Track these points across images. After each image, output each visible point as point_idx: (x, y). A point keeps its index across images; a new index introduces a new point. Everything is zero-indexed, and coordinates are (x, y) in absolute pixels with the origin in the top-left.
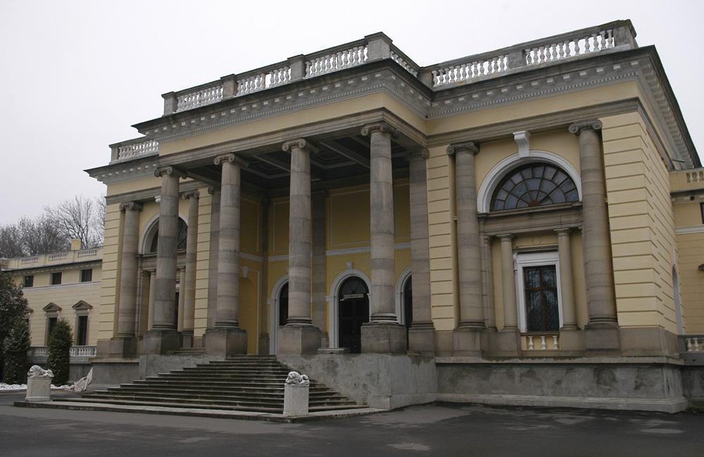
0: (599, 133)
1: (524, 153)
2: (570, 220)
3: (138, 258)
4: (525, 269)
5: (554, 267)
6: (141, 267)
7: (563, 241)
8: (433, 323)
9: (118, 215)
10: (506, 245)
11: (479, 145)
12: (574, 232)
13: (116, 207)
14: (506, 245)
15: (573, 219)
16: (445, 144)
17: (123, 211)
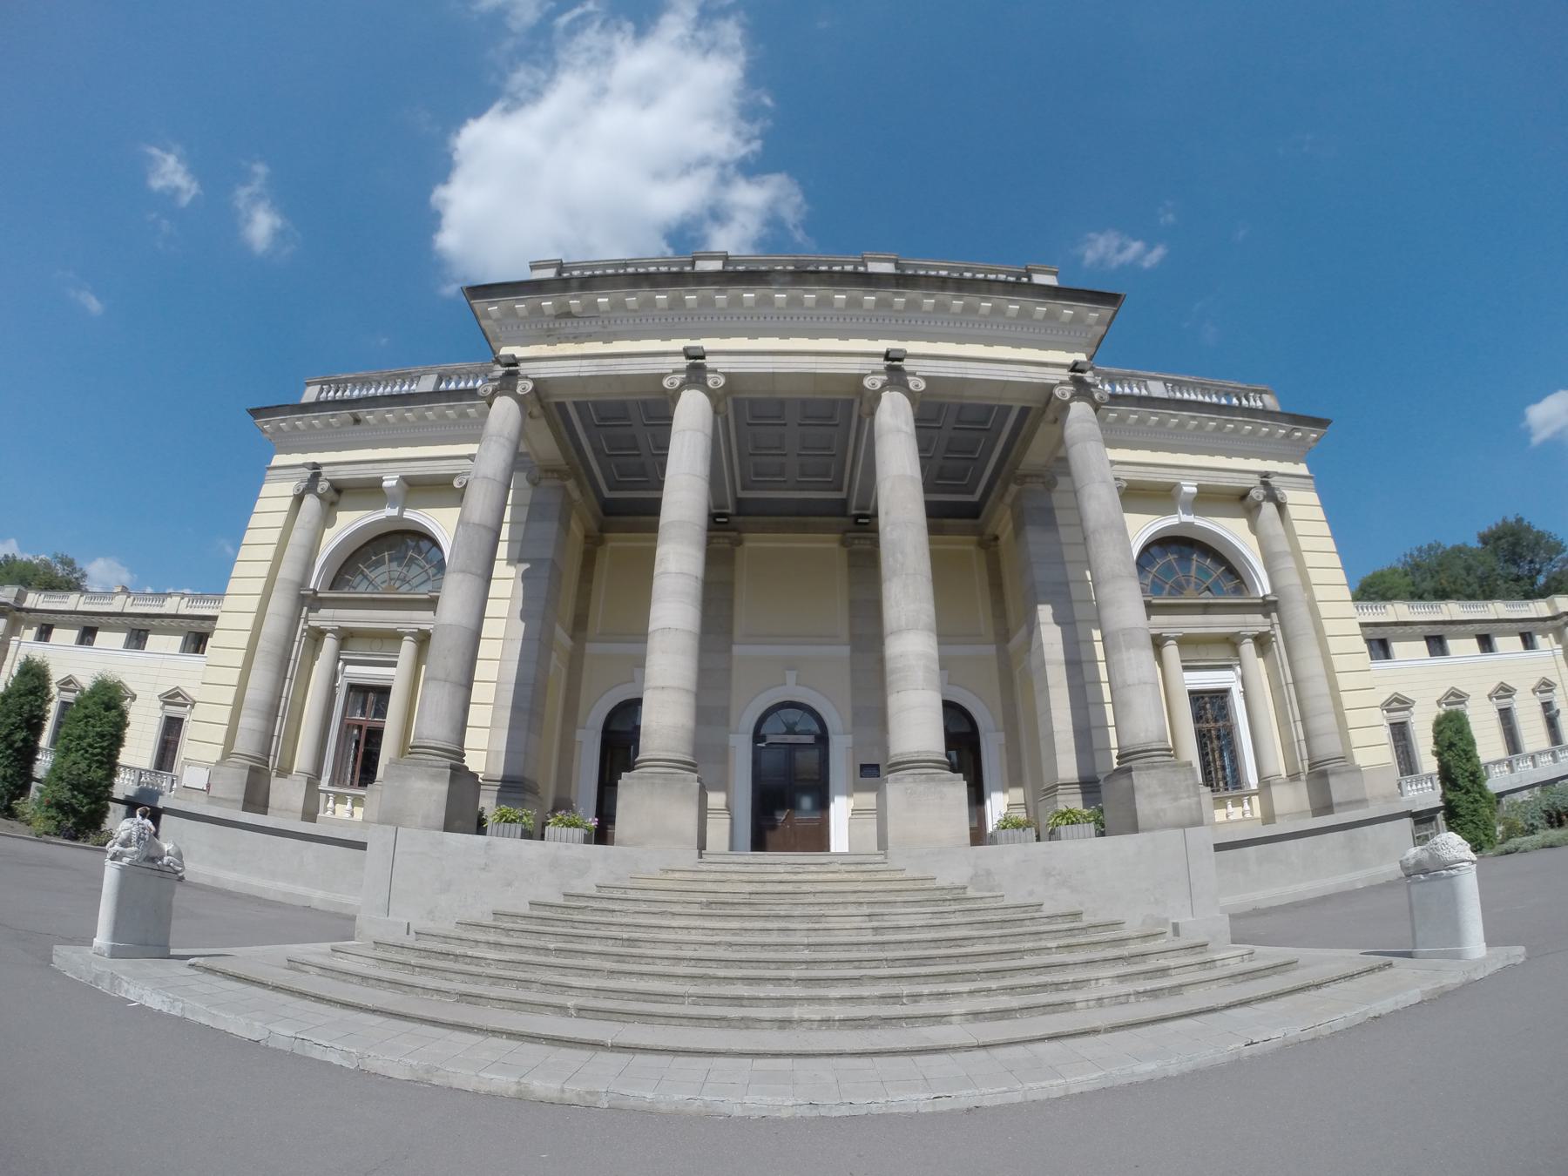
0: (1281, 507)
2: (1257, 622)
3: (307, 601)
4: (1191, 693)
6: (306, 621)
7: (1248, 649)
9: (286, 504)
10: (1171, 652)
12: (1262, 643)
13: (289, 488)
14: (1171, 652)
15: (1259, 618)
17: (299, 499)
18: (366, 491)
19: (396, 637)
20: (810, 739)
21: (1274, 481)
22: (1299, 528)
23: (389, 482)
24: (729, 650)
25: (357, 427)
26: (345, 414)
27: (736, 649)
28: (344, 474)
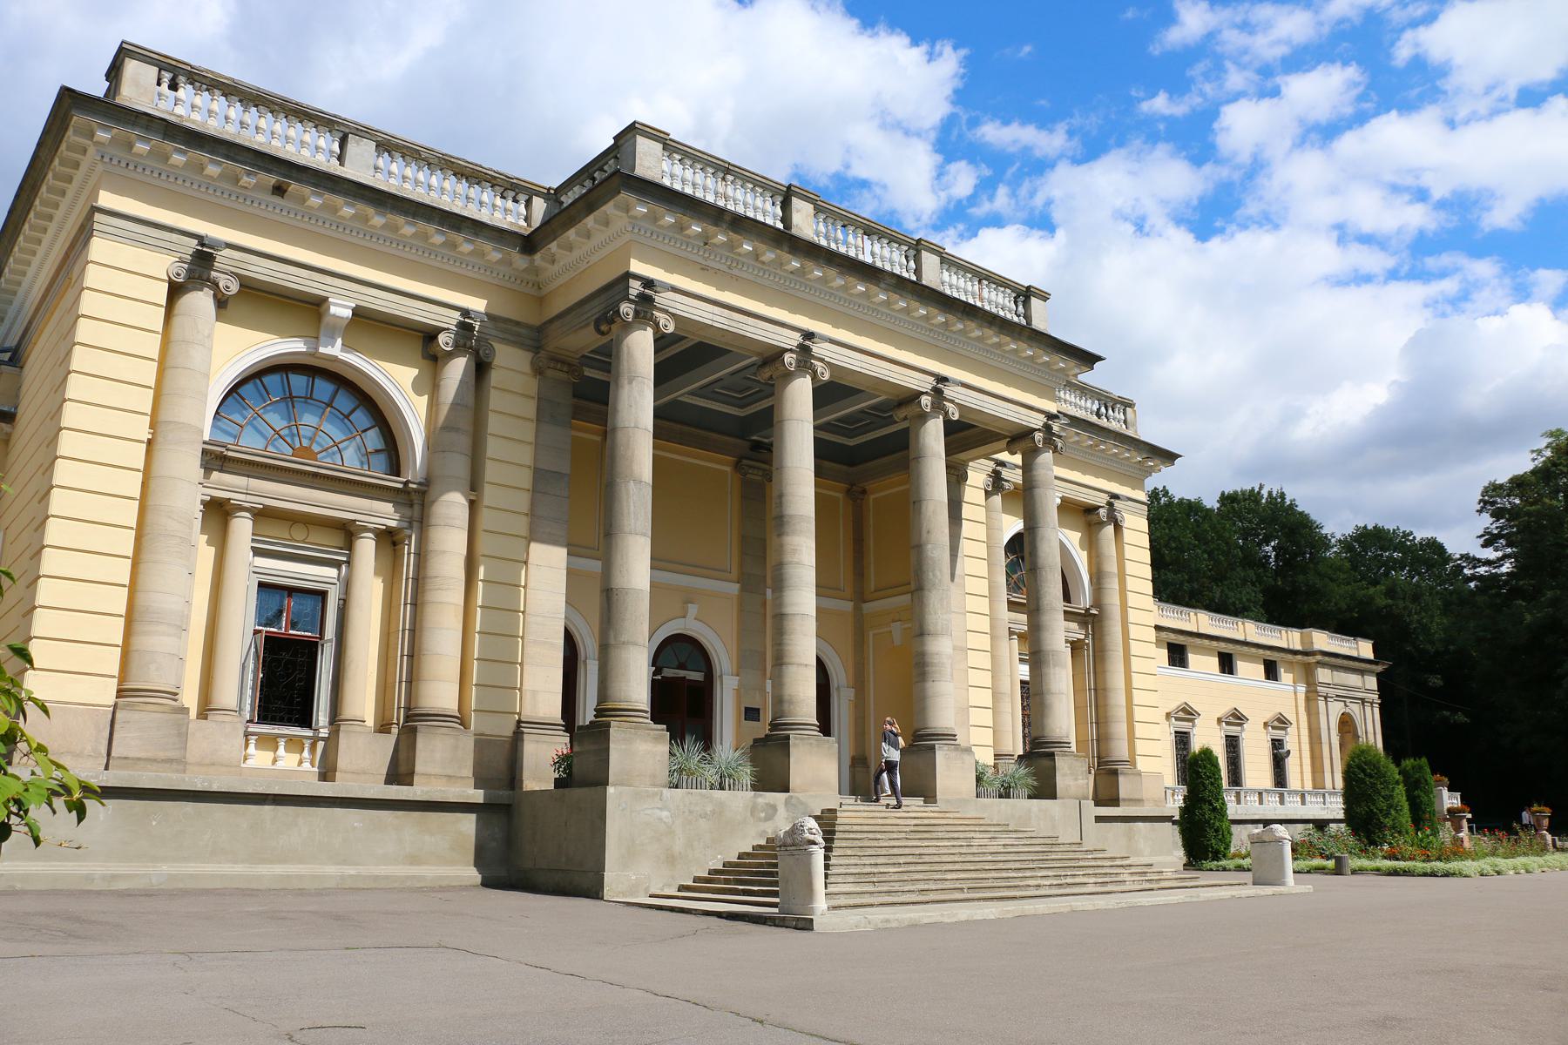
13: (165, 264)
17: (175, 291)
18: (306, 309)
19: (347, 532)
20: (696, 676)
21: (1117, 504)
22: (1129, 552)
23: (341, 309)
25: (276, 200)
26: (272, 179)
28: (262, 271)
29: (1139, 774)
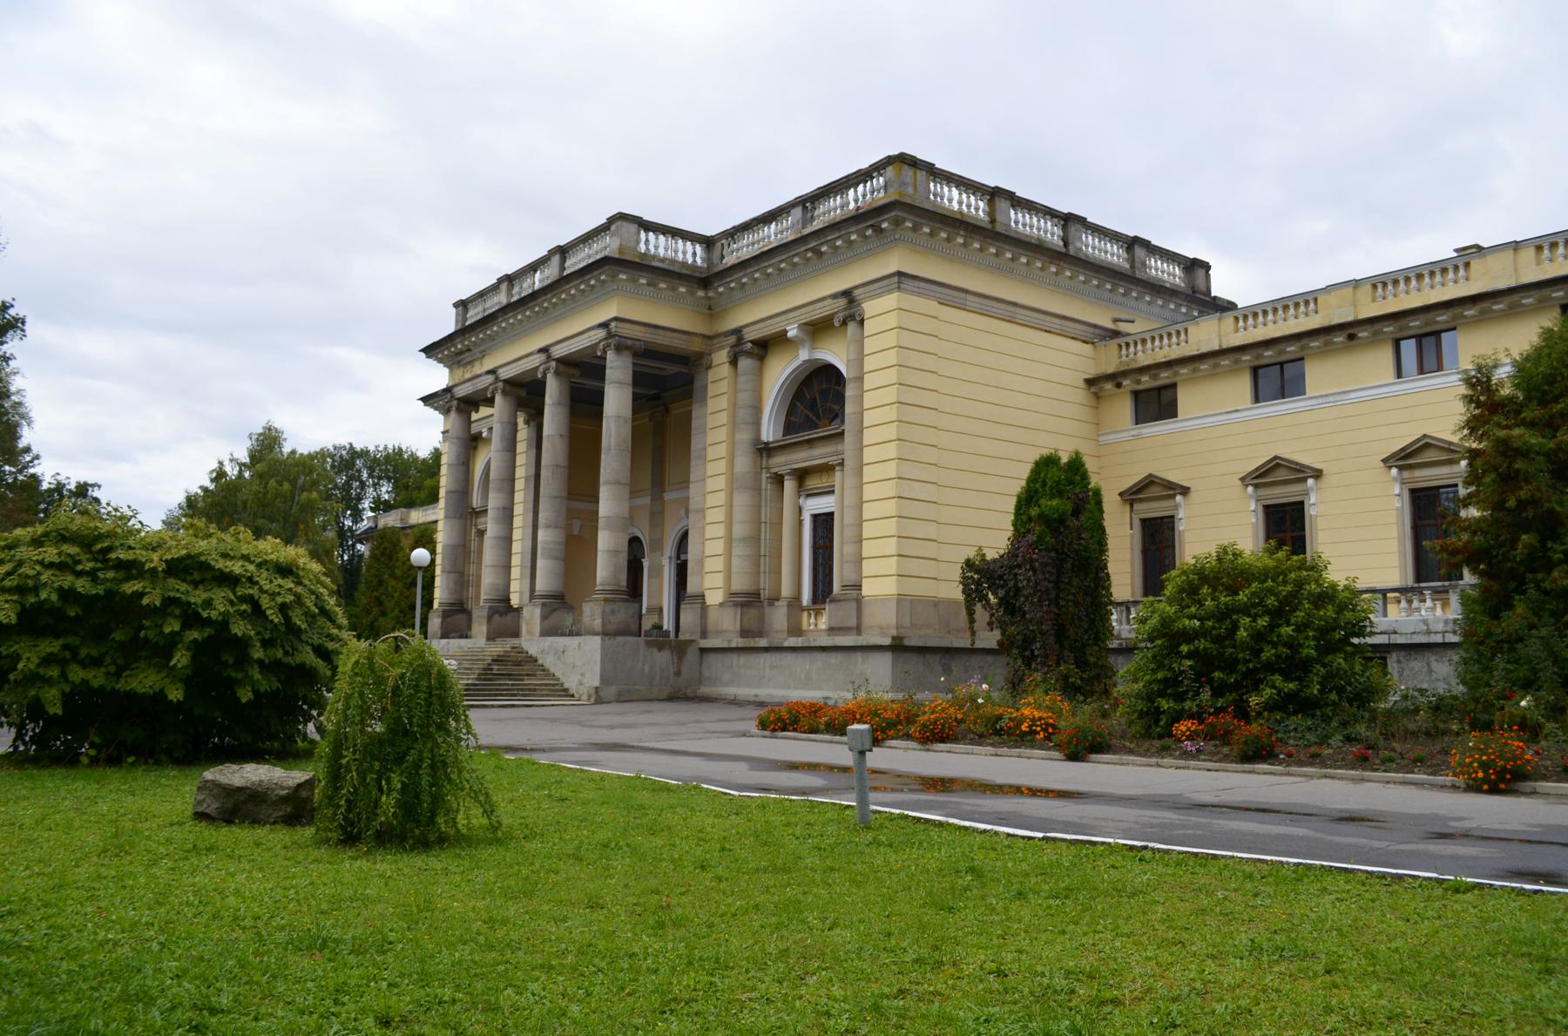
1: (804, 355)
4: (815, 517)
5: (832, 514)
8: (703, 596)
10: (789, 485)
11: (764, 347)
14: (789, 485)
16: (722, 348)
24: (661, 498)
27: (667, 496)
29: (859, 601)
